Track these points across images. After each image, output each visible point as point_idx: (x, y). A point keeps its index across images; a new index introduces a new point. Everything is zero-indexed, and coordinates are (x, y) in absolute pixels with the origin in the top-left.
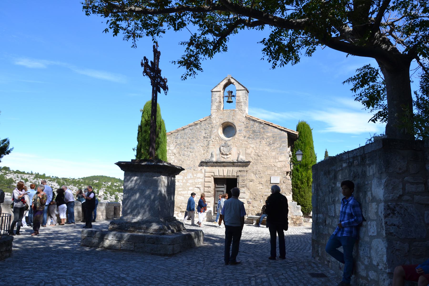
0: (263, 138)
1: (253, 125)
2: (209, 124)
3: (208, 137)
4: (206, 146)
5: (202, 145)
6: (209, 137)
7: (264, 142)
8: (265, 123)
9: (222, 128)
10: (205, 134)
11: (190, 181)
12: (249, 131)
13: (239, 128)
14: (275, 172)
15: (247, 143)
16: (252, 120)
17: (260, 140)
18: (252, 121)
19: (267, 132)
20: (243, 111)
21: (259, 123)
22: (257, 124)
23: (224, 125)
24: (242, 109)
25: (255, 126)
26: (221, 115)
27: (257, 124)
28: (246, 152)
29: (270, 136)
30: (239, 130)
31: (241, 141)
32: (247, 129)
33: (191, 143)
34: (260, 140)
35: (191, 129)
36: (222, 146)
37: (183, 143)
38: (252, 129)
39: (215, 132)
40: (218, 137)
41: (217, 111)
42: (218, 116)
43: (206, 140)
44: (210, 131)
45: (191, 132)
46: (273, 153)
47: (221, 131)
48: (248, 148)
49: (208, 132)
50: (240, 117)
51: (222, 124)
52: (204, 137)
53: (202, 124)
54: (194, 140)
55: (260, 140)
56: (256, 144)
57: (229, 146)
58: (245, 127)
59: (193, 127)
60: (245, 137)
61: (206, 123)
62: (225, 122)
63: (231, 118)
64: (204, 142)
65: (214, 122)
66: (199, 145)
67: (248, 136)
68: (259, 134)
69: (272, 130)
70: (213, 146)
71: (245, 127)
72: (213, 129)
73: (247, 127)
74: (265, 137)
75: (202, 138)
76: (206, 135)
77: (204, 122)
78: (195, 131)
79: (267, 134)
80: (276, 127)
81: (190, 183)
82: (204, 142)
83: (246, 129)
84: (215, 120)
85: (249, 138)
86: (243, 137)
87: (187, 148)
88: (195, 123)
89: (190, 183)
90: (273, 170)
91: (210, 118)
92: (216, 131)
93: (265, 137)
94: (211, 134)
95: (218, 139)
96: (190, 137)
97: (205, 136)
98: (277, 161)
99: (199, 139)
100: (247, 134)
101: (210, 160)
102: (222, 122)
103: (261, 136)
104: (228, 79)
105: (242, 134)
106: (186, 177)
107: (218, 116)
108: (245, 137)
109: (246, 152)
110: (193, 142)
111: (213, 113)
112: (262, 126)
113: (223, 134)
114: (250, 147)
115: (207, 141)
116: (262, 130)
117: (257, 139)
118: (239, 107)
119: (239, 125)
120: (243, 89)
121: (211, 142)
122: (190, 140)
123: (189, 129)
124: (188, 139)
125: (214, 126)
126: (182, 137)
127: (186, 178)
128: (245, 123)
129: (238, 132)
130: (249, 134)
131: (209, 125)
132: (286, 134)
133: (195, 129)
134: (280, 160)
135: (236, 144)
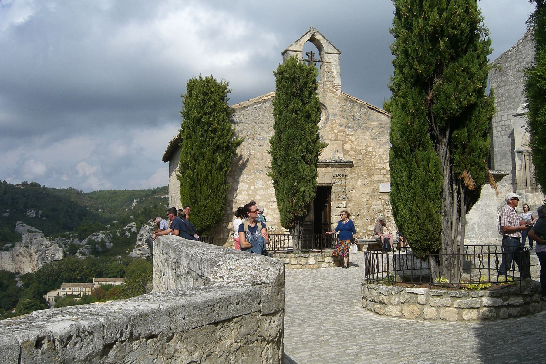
0: (367, 128)
11: (262, 192)
14: (383, 177)
28: (343, 148)
30: (333, 115)
34: (363, 131)
46: (380, 150)
48: (347, 143)
60: (342, 125)
69: (377, 117)
73: (344, 111)
78: (263, 112)
81: (261, 196)
85: (347, 126)
87: (253, 139)
89: (261, 196)
90: (380, 174)
103: (364, 125)
104: (312, 33)
106: (254, 185)
109: (343, 148)
114: (350, 140)
116: (364, 116)
120: (336, 52)
124: (253, 123)
127: (253, 187)
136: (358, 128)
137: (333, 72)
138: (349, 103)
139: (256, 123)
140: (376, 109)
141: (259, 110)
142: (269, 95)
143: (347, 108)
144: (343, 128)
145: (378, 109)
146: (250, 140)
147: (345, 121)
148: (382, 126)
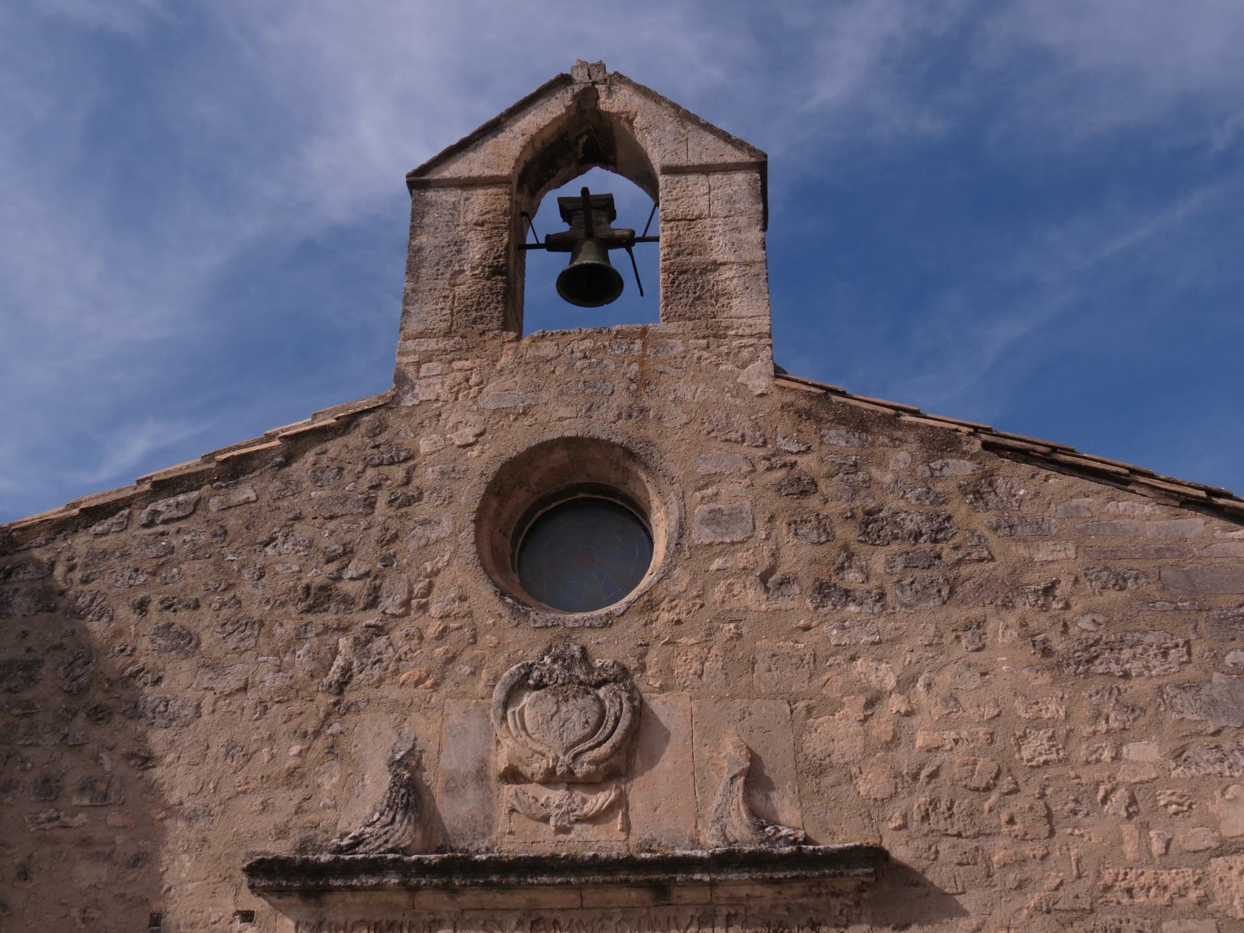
16: (841, 421)
28: (798, 747)
46: (1132, 751)
54: (182, 618)
59: (194, 495)
62: (547, 447)
85: (823, 590)
94: (388, 561)
98: (1203, 838)
101: (358, 841)
112: (960, 468)
116: (959, 509)
120: (732, 155)
134: (1227, 832)
136: (922, 594)
137: (716, 265)
138: (837, 438)
139: (142, 607)
141: (182, 525)
145: (1071, 452)
146: (80, 720)
147: (806, 550)
148: (1120, 566)
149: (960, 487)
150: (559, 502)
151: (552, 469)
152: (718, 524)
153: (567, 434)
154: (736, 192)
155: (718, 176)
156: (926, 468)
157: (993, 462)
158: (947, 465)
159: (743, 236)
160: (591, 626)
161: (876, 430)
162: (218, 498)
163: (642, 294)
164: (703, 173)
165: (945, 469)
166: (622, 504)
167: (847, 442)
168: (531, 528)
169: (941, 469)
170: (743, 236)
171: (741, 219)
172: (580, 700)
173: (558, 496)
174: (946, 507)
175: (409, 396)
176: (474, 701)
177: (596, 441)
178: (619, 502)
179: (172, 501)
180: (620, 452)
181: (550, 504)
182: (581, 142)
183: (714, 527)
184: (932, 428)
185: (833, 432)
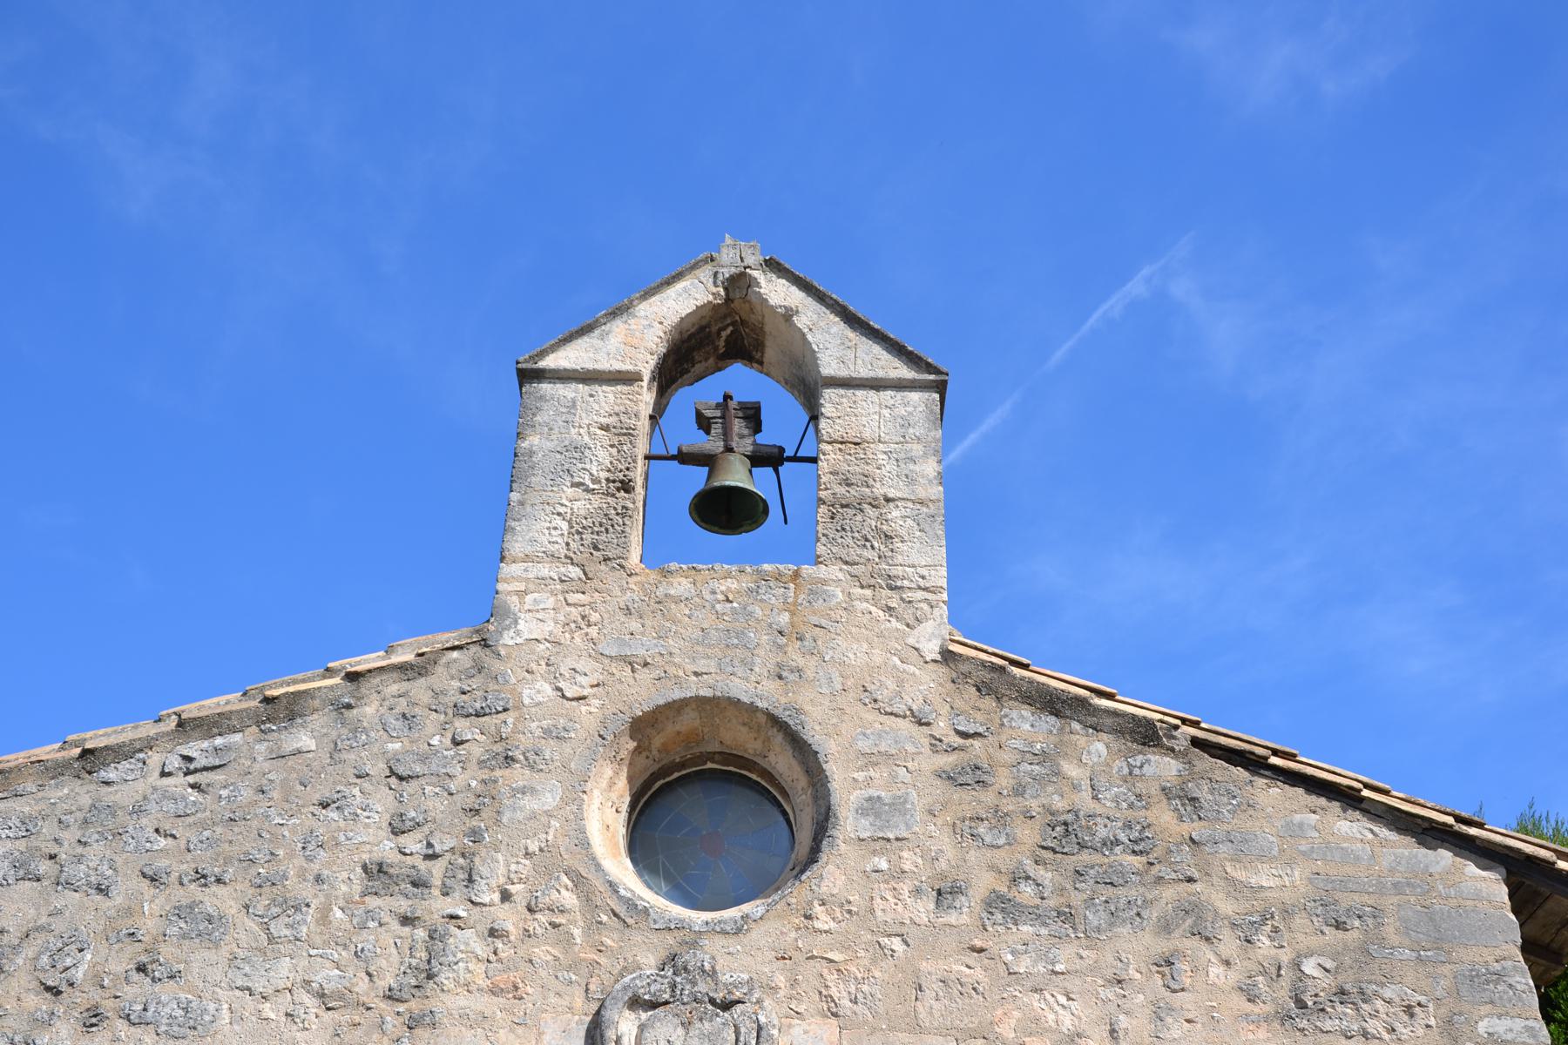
1: (1043, 757)
2: (459, 711)
3: (437, 870)
4: (391, 996)
5: (327, 976)
6: (449, 874)
7: (1216, 971)
8: (1196, 742)
9: (622, 783)
10: (396, 832)
12: (1000, 819)
13: (860, 776)
15: (979, 973)
17: (1155, 944)
18: (1026, 712)
19: (1244, 849)
20: (907, 595)
21: (1118, 732)
22: (1100, 747)
23: (657, 742)
24: (898, 571)
25: (1071, 770)
26: (634, 625)
27: (1099, 747)
29: (1287, 896)
31: (896, 944)
32: (968, 801)
33: (167, 951)
34: (1162, 946)
35: (201, 761)
36: (636, 1003)
37: (29, 951)
38: (1034, 805)
39: (533, 816)
40: (579, 881)
41: (575, 572)
42: (593, 631)
43: (403, 905)
44: (471, 801)
45: (193, 796)
47: (610, 812)
49: (437, 805)
50: (878, 657)
51: (642, 727)
52: (377, 872)
53: (369, 711)
55: (1155, 944)
56: (1109, 993)
57: (726, 1006)
58: (949, 777)
59: (237, 737)
60: (956, 891)
61: (425, 698)
62: (677, 707)
63: (765, 660)
64: (365, 940)
65: (538, 691)
66: (284, 970)
67: (983, 883)
68: (1137, 862)
69: (1295, 832)
70: (495, 991)
71: (949, 777)
72: (518, 775)
73: (971, 777)
74: (1227, 907)
75: (348, 882)
76: (413, 842)
77: (394, 688)
78: (246, 794)
79: (1240, 875)
80: (1348, 798)
82: (365, 940)
83: (958, 795)
84: (554, 677)
85: (997, 904)
86: (917, 892)
88: (269, 693)
91: (484, 644)
92: (549, 799)
93: (1227, 907)
94: (476, 836)
95: (569, 899)
96: (162, 863)
97: (392, 857)
99: (307, 891)
100: (973, 856)
102: (644, 694)
103: (1169, 893)
105: (909, 860)
107: (593, 631)
108: (945, 894)
110: (208, 928)
111: (522, 594)
112: (1162, 767)
113: (628, 862)
115: (406, 920)
116: (1164, 817)
117: (1125, 930)
118: (854, 553)
119: (864, 745)
121: (467, 941)
122: (154, 905)
123: (174, 763)
125: (525, 741)
126: (44, 867)
128: (942, 727)
129: (849, 824)
130: (1003, 859)
131: (463, 727)
132: (1491, 887)
133: (263, 764)
135: (832, 978)
140: (1274, 760)
142: (329, 672)
143: (1007, 757)
144: (962, 915)
149: (1164, 789)
150: (684, 772)
151: (679, 733)
152: (877, 815)
153: (702, 693)
154: (910, 414)
155: (889, 393)
156: (1124, 764)
157: (1205, 762)
158: (1148, 761)
159: (917, 468)
160: (724, 933)
161: (1068, 713)
162: (266, 744)
163: (786, 522)
164: (872, 388)
165: (1146, 766)
166: (759, 779)
167: (1032, 726)
168: (646, 803)
169: (1141, 767)
170: (917, 468)
171: (915, 447)
172: (707, 1024)
173: (683, 765)
174: (1148, 813)
175: (511, 633)
176: (577, 1017)
177: (737, 703)
178: (754, 777)
179: (205, 744)
180: (763, 719)
181: (672, 774)
182: (724, 334)
183: (871, 819)
184: (1134, 716)
185: (1014, 714)
